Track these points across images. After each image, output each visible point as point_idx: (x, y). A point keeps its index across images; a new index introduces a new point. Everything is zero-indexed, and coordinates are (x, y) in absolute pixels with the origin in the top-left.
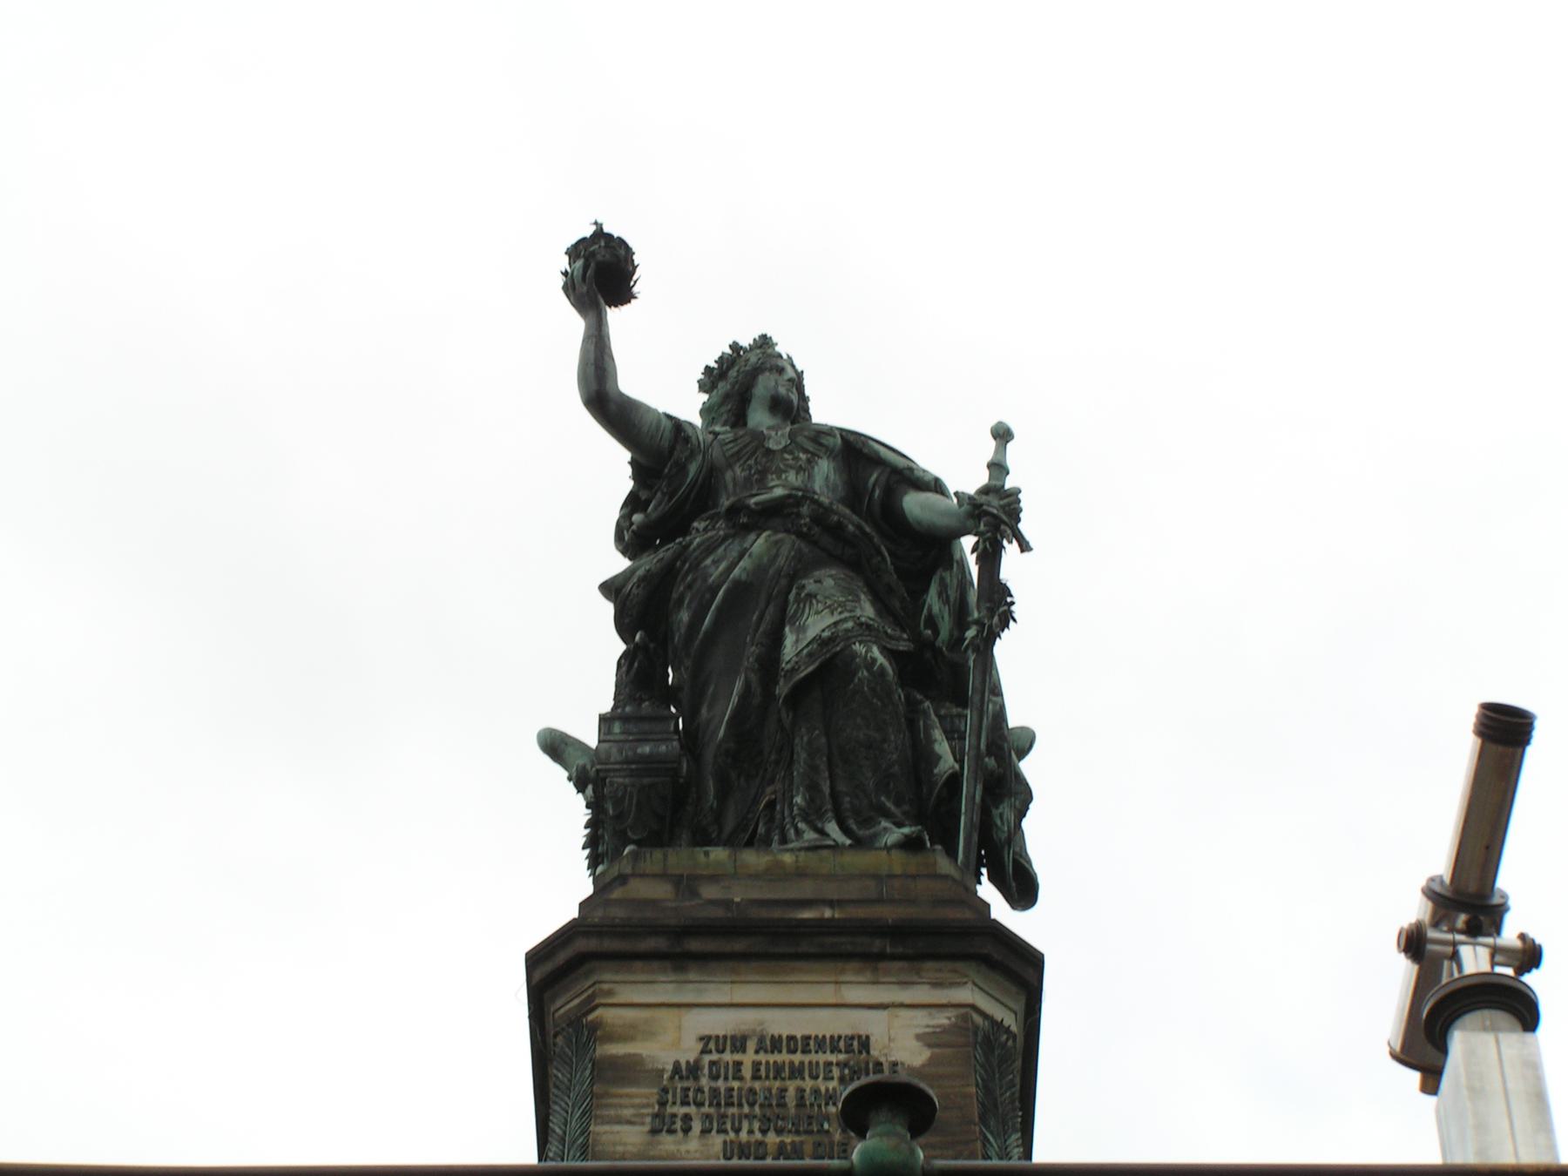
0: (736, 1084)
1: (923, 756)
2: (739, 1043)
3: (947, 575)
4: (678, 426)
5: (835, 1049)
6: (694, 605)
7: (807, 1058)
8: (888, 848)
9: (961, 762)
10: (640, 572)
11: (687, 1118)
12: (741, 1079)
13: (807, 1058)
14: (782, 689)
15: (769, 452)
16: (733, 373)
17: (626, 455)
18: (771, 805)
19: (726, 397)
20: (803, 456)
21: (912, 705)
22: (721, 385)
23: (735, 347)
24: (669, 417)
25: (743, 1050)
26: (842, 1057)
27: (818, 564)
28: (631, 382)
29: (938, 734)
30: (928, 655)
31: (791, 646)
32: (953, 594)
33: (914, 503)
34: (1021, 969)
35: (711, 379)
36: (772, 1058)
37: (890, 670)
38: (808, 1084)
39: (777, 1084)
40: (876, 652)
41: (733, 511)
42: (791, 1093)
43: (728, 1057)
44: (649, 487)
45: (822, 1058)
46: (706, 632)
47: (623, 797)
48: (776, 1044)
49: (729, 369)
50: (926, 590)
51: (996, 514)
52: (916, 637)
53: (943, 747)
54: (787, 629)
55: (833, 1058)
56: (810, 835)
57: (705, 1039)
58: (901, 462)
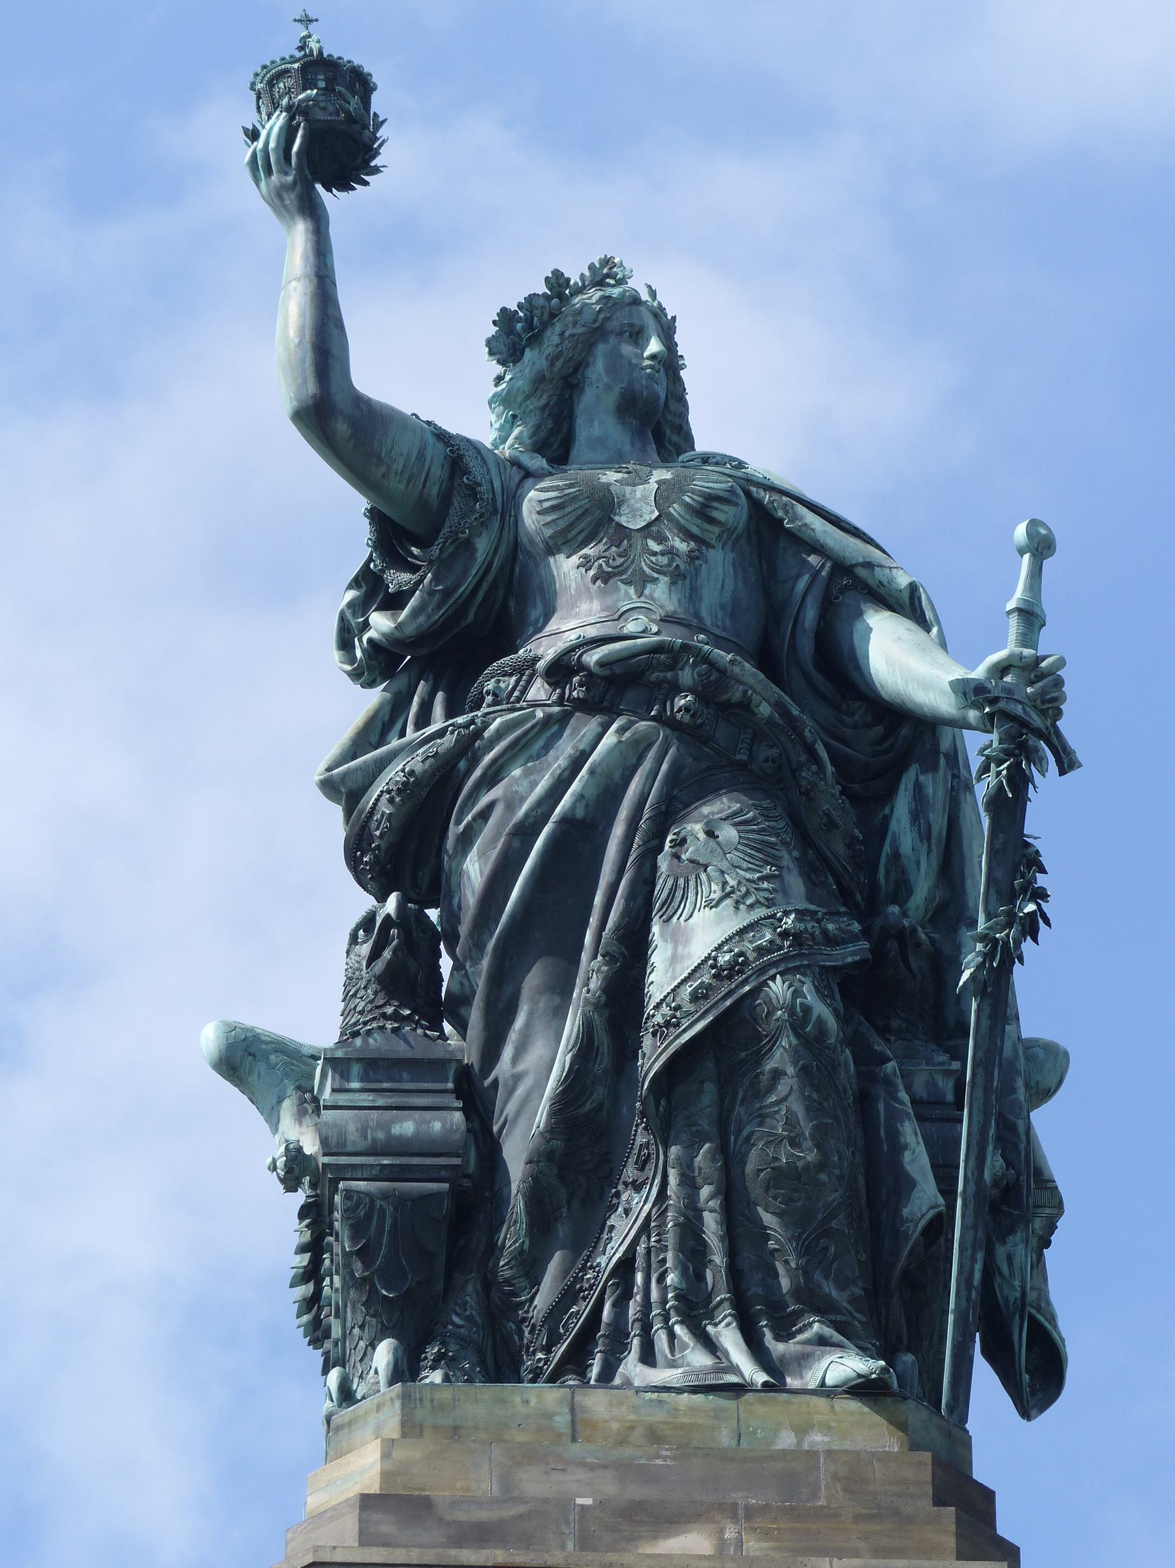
1: (881, 1181)
3: (926, 780)
4: (456, 453)
6: (494, 854)
8: (824, 1390)
10: (393, 774)
14: (652, 1057)
15: (623, 532)
16: (552, 337)
17: (360, 503)
18: (626, 1266)
19: (539, 381)
20: (682, 546)
21: (868, 1061)
22: (528, 354)
23: (557, 281)
24: (442, 436)
27: (705, 789)
28: (374, 375)
29: (910, 1132)
31: (663, 975)
32: (938, 821)
35: (515, 335)
37: (832, 1022)
40: (810, 995)
41: (561, 670)
46: (512, 917)
47: (369, 1215)
49: (545, 325)
53: (917, 1159)
54: (656, 929)
56: (699, 1359)
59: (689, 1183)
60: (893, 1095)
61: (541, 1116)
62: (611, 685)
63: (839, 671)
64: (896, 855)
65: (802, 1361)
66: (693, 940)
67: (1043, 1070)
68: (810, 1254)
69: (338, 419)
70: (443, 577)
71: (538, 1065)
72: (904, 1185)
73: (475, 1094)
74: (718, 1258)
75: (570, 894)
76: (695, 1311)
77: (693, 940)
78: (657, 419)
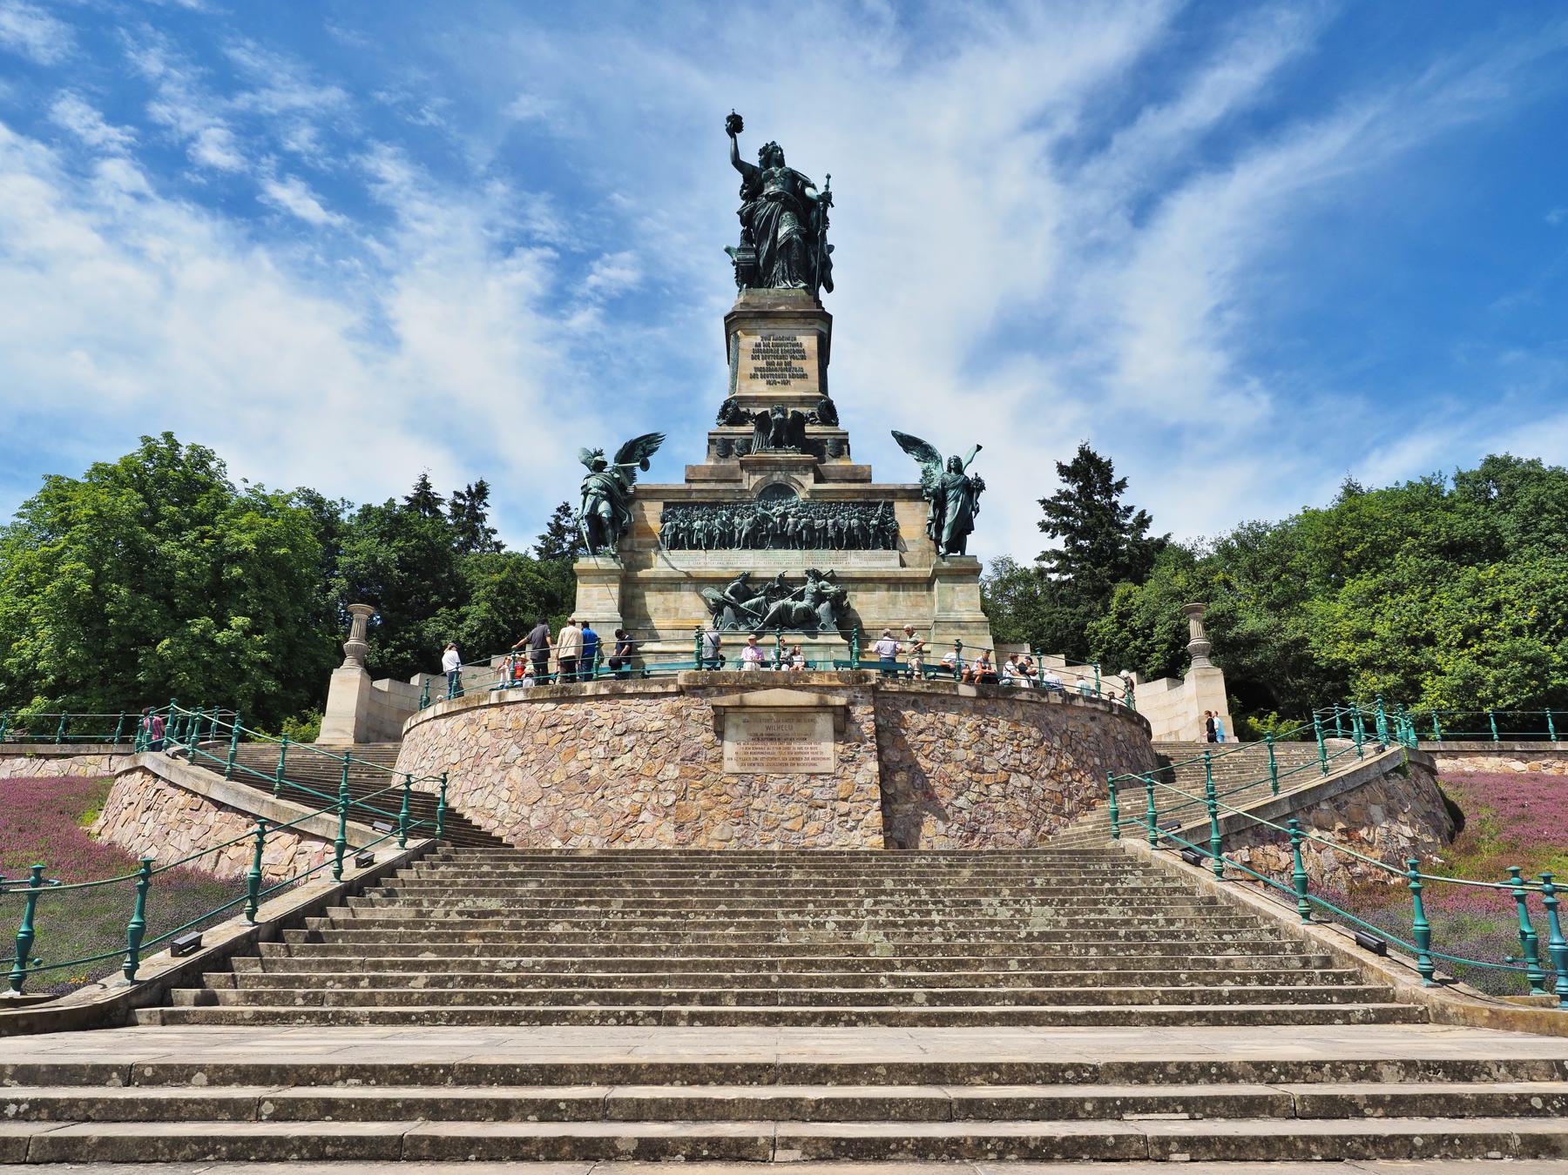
28: (742, 158)
33: (809, 191)
34: (828, 319)
35: (762, 152)
51: (826, 198)
62: (771, 198)
66: (783, 231)
67: (831, 248)
69: (737, 163)
70: (753, 182)
71: (766, 247)
73: (757, 252)
75: (769, 225)
77: (783, 231)
78: (780, 162)
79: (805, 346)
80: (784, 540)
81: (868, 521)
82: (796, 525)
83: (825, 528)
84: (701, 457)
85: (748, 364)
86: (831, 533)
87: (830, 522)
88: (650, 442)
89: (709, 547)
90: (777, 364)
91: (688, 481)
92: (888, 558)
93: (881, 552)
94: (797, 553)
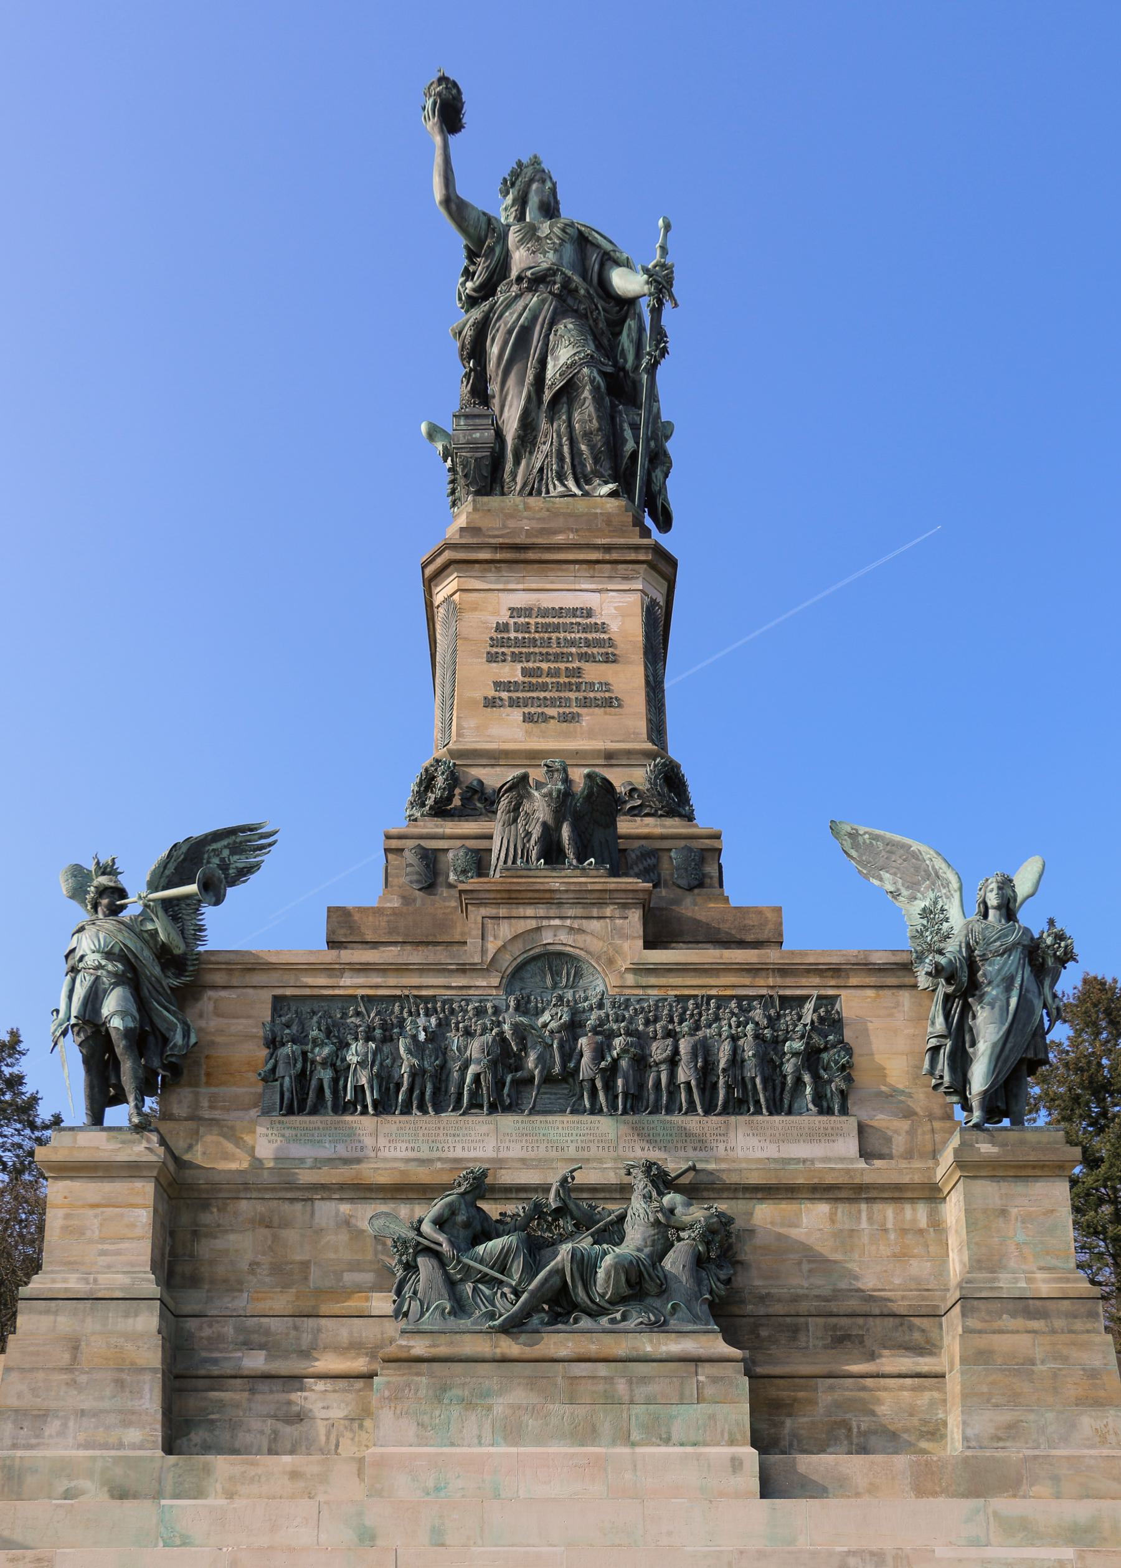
0: (527, 636)
2: (527, 611)
5: (575, 616)
7: (561, 620)
9: (637, 443)
11: (503, 654)
12: (530, 632)
13: (561, 620)
18: (541, 470)
21: (613, 407)
25: (530, 616)
26: (578, 620)
29: (626, 426)
30: (622, 374)
36: (543, 621)
38: (562, 635)
39: (546, 635)
42: (554, 641)
43: (522, 620)
44: (475, 264)
45: (568, 620)
48: (545, 613)
50: (620, 333)
52: (615, 364)
53: (628, 433)
55: (574, 620)
57: (512, 609)
58: (608, 247)
59: (559, 437)
60: (621, 415)
61: (515, 425)
63: (604, 286)
64: (623, 350)
65: (595, 489)
68: (596, 460)
72: (624, 441)
74: (568, 460)
76: (561, 477)
79: (614, 627)
80: (564, 1090)
81: (777, 1043)
82: (600, 1053)
83: (673, 1061)
84: (365, 885)
85: (480, 676)
86: (684, 1074)
87: (684, 1046)
88: (237, 849)
89: (383, 1107)
90: (547, 664)
91: (332, 944)
92: (829, 1136)
93: (810, 1120)
94: (604, 1125)
